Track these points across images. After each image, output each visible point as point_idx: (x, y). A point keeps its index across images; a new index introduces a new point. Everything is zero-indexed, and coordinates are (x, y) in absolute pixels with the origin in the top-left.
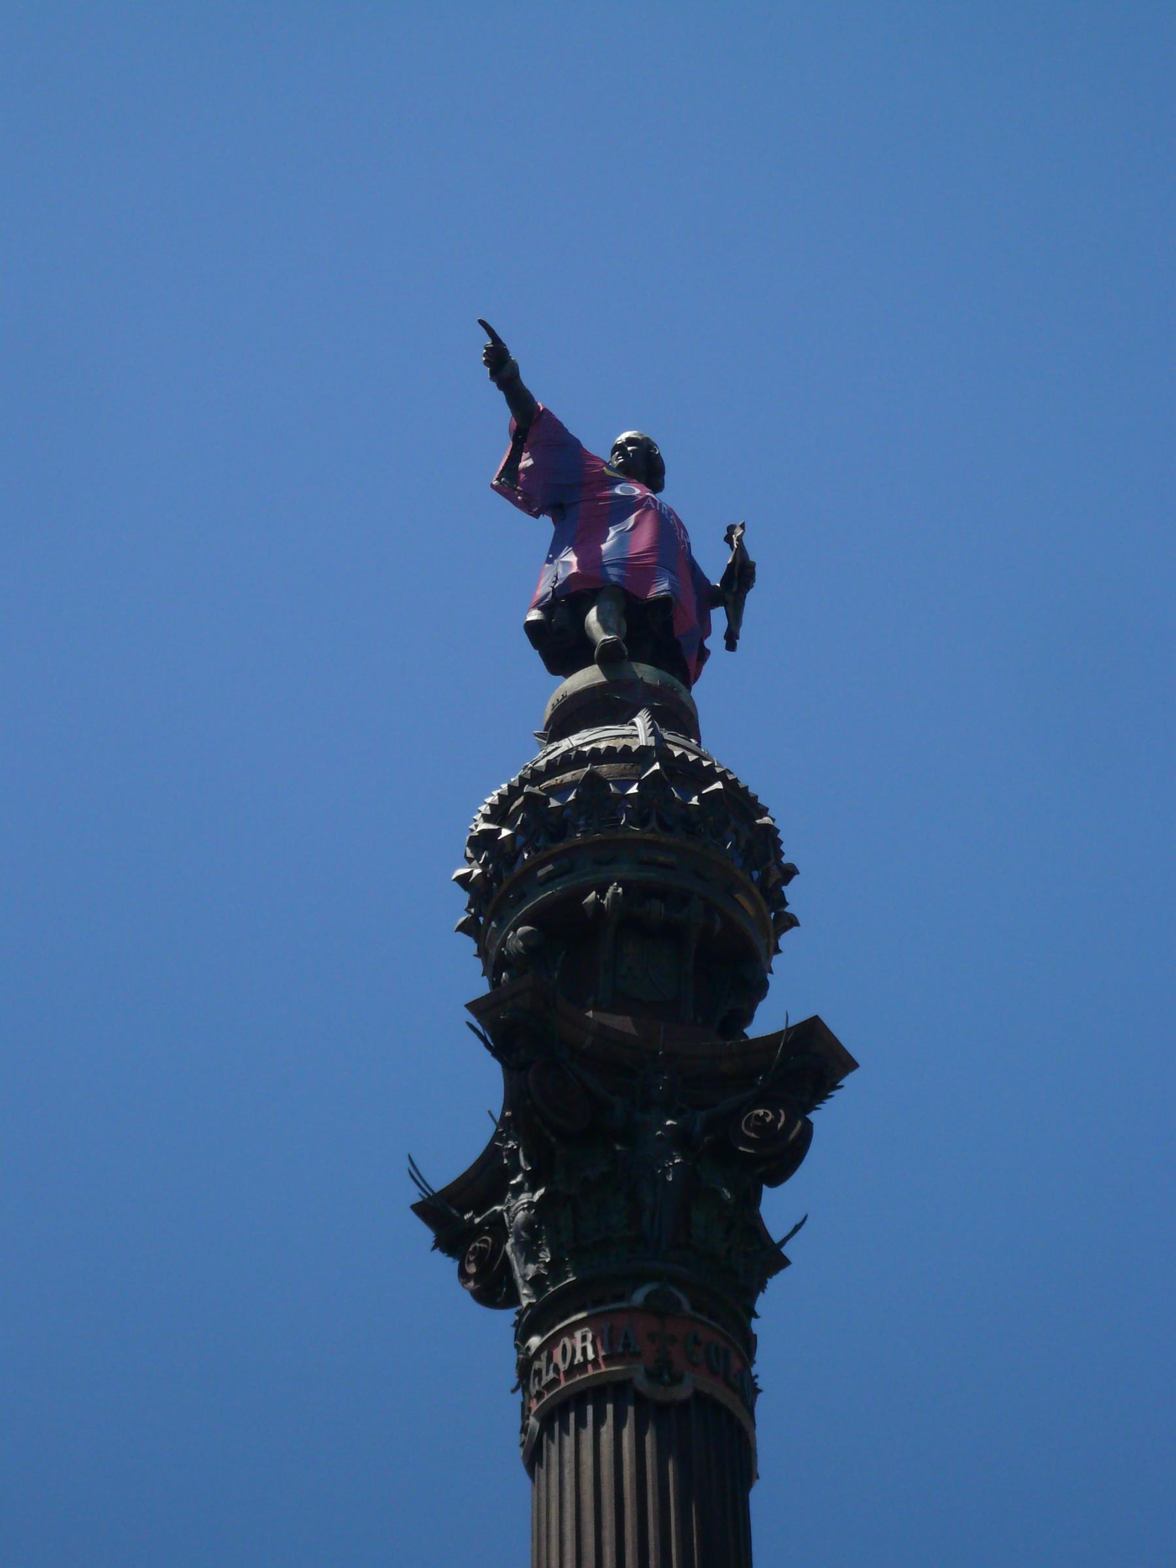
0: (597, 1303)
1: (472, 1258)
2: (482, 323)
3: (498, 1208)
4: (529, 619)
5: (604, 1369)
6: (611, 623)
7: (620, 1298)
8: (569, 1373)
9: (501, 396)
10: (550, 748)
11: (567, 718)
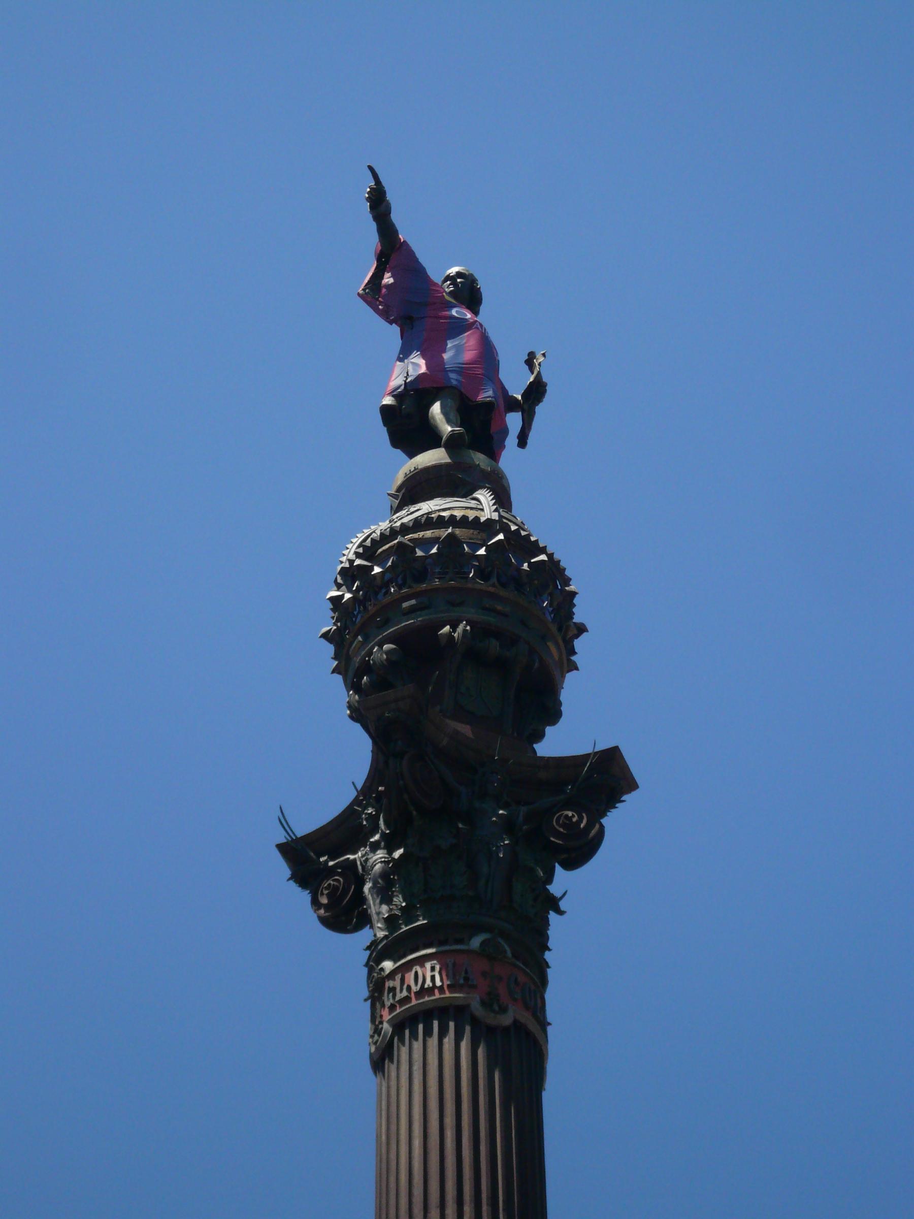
0: (441, 943)
1: (326, 892)
2: (371, 168)
3: (352, 857)
4: (384, 403)
5: (448, 995)
6: (452, 416)
7: (460, 941)
9: (374, 226)
10: (412, 509)
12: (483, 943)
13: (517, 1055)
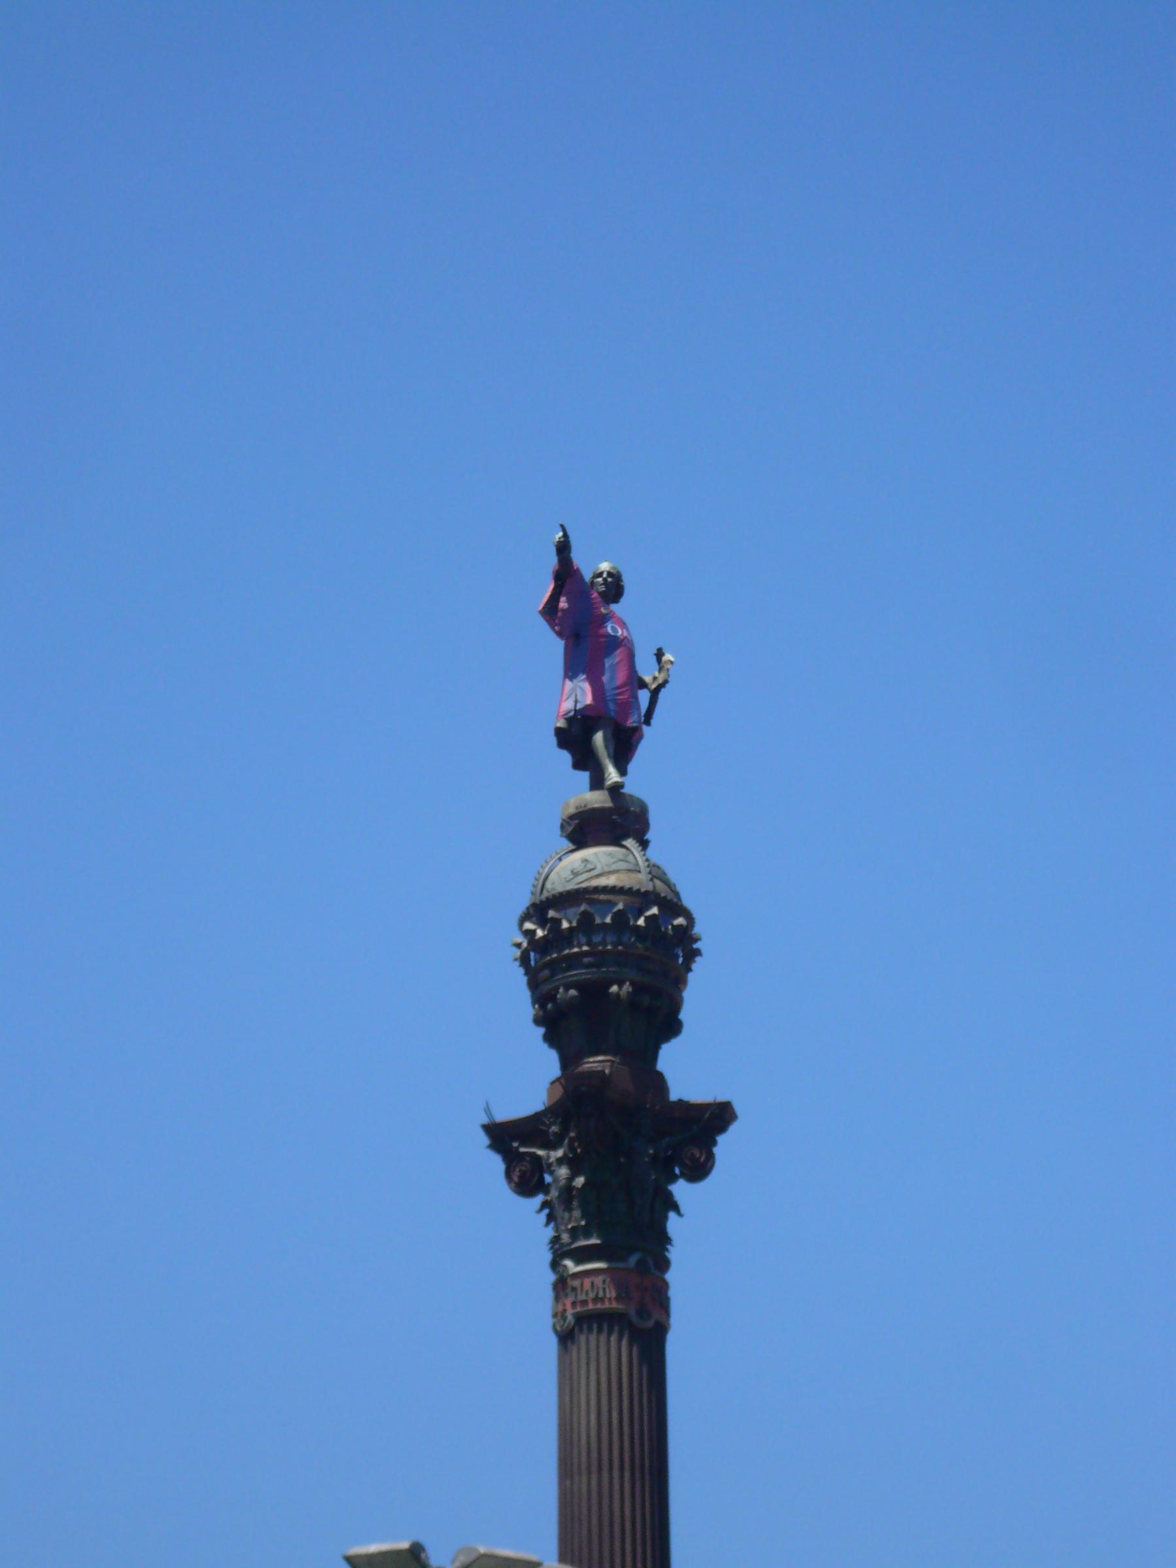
3: (540, 1153)
4: (559, 725)
8: (597, 1299)
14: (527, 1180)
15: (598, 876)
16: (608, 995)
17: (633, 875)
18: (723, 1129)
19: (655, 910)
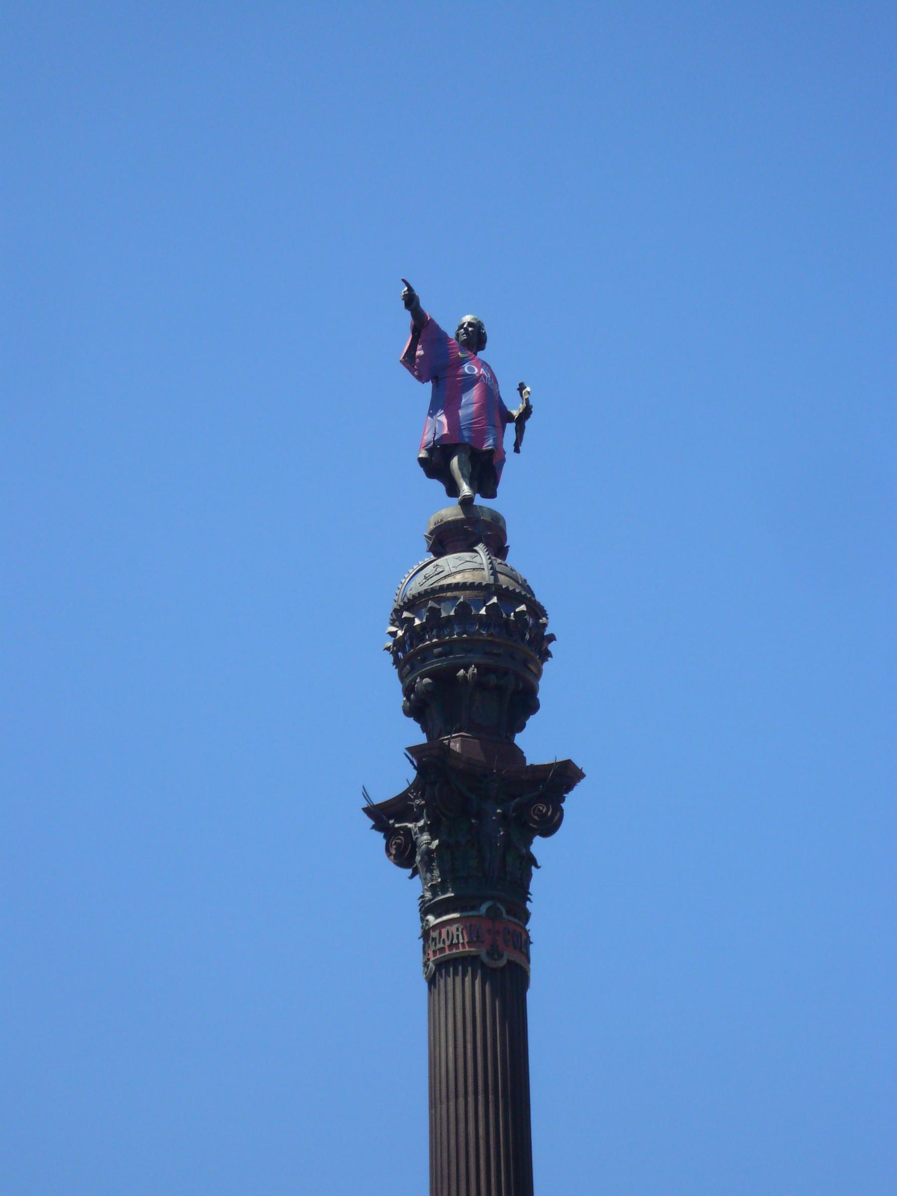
2: (403, 280)
3: (410, 825)
4: (420, 456)
5: (467, 949)
6: (465, 472)
7: (473, 908)
8: (451, 946)
11: (444, 540)
12: (488, 909)
13: (508, 983)
14: (403, 854)
15: (445, 577)
16: (456, 678)
17: (476, 572)
18: (569, 788)
19: (495, 600)
